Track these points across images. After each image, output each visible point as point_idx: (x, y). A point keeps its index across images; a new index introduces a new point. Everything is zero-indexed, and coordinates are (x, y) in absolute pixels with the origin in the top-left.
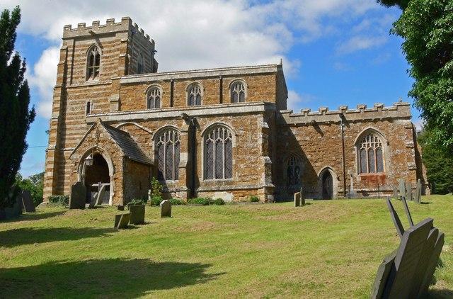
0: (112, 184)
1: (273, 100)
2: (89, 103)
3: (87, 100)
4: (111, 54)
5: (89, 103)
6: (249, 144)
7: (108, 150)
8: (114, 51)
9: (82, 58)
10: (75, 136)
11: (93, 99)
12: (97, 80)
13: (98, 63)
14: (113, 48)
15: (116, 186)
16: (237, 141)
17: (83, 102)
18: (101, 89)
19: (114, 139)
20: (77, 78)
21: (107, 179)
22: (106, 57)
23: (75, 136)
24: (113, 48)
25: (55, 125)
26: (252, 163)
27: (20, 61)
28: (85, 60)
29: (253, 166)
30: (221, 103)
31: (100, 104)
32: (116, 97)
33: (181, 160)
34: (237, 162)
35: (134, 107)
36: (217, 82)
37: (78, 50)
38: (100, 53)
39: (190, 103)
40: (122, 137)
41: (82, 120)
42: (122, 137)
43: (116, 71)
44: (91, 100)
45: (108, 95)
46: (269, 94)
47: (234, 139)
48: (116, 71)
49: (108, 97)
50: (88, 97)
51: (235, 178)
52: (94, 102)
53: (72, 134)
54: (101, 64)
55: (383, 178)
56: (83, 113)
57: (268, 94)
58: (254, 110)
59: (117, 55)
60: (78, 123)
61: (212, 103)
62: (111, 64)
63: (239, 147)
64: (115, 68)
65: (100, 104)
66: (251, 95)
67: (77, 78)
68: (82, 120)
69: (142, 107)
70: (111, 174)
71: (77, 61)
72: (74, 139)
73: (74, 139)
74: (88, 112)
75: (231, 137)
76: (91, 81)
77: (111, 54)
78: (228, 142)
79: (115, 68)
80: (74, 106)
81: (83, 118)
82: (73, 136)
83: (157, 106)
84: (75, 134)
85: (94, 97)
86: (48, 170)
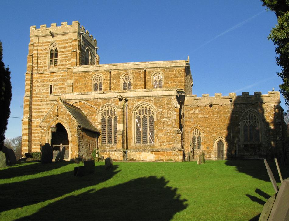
0: (70, 145)
1: (182, 88)
2: (51, 86)
3: (50, 84)
4: (66, 49)
5: (51, 86)
6: (166, 119)
7: (67, 120)
8: (68, 47)
9: (45, 52)
10: (42, 110)
11: (54, 83)
12: (56, 69)
13: (56, 56)
14: (67, 45)
15: (73, 147)
16: (158, 117)
17: (47, 85)
18: (59, 76)
19: (71, 113)
20: (42, 67)
21: (67, 142)
22: (62, 52)
23: (42, 110)
24: (67, 45)
25: (27, 101)
26: (168, 132)
27: (76, 168)
28: (47, 53)
29: (169, 135)
30: (145, 88)
31: (59, 87)
32: (70, 82)
33: (118, 129)
34: (157, 132)
35: (84, 90)
36: (143, 72)
37: (42, 46)
38: (58, 49)
39: (124, 88)
40: (77, 112)
41: (47, 99)
42: (77, 112)
43: (70, 62)
44: (52, 84)
45: (65, 80)
46: (180, 83)
47: (155, 116)
48: (70, 62)
49: (64, 82)
50: (50, 82)
51: (157, 144)
52: (55, 85)
53: (38, 105)
54: (59, 57)
55: (259, 146)
56: (47, 93)
57: (179, 82)
58: (169, 94)
59: (70, 50)
60: (44, 100)
61: (139, 88)
62: (66, 57)
63: (159, 121)
64: (69, 60)
65: (59, 87)
66: (166, 83)
67: (42, 67)
68: (47, 99)
69: (90, 90)
70: (69, 138)
71: (41, 54)
72: (42, 112)
73: (42, 112)
74: (51, 92)
75: (153, 113)
76: (52, 69)
77: (66, 49)
78: (151, 118)
79: (69, 60)
80: (41, 88)
81: (47, 97)
82: (41, 110)
83: (100, 89)
84: (42, 109)
85: (55, 82)
86: (25, 134)
